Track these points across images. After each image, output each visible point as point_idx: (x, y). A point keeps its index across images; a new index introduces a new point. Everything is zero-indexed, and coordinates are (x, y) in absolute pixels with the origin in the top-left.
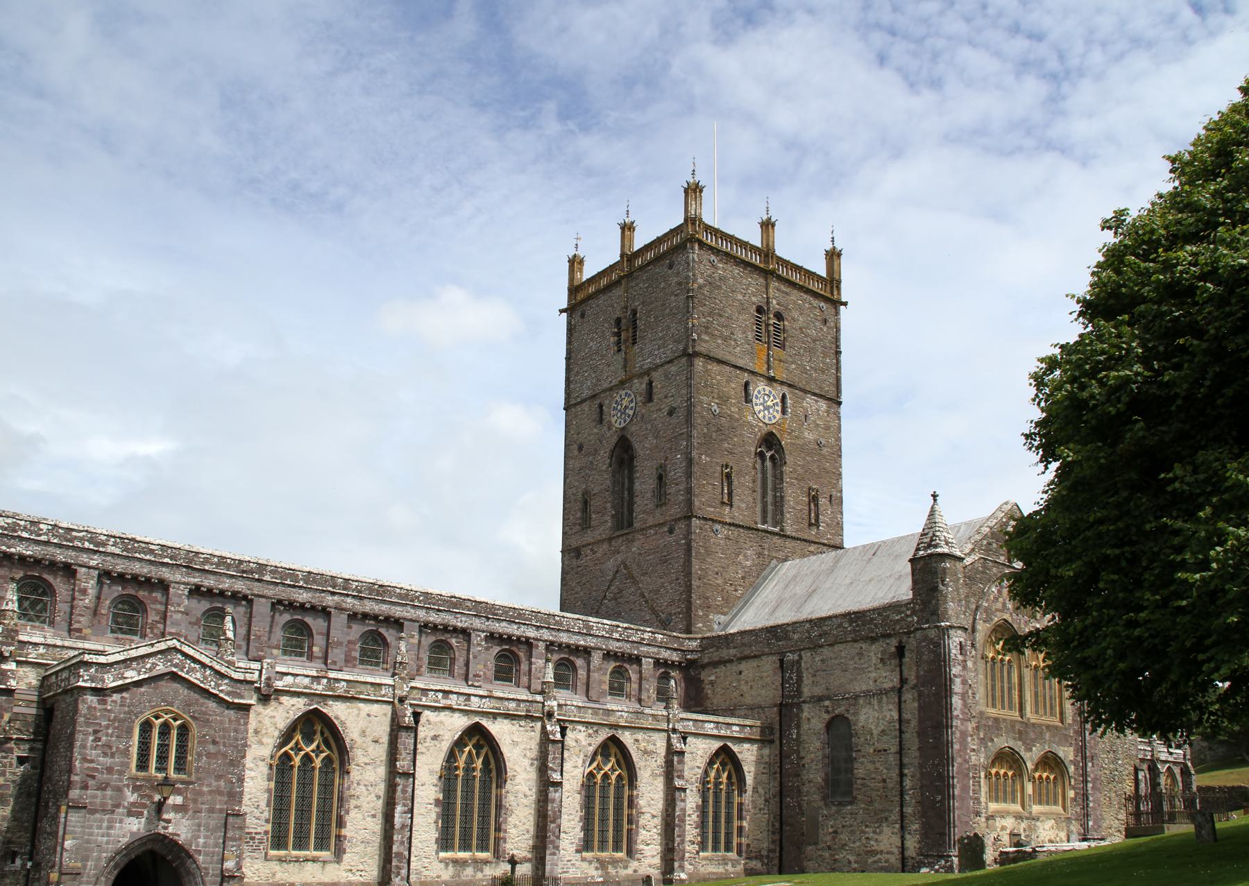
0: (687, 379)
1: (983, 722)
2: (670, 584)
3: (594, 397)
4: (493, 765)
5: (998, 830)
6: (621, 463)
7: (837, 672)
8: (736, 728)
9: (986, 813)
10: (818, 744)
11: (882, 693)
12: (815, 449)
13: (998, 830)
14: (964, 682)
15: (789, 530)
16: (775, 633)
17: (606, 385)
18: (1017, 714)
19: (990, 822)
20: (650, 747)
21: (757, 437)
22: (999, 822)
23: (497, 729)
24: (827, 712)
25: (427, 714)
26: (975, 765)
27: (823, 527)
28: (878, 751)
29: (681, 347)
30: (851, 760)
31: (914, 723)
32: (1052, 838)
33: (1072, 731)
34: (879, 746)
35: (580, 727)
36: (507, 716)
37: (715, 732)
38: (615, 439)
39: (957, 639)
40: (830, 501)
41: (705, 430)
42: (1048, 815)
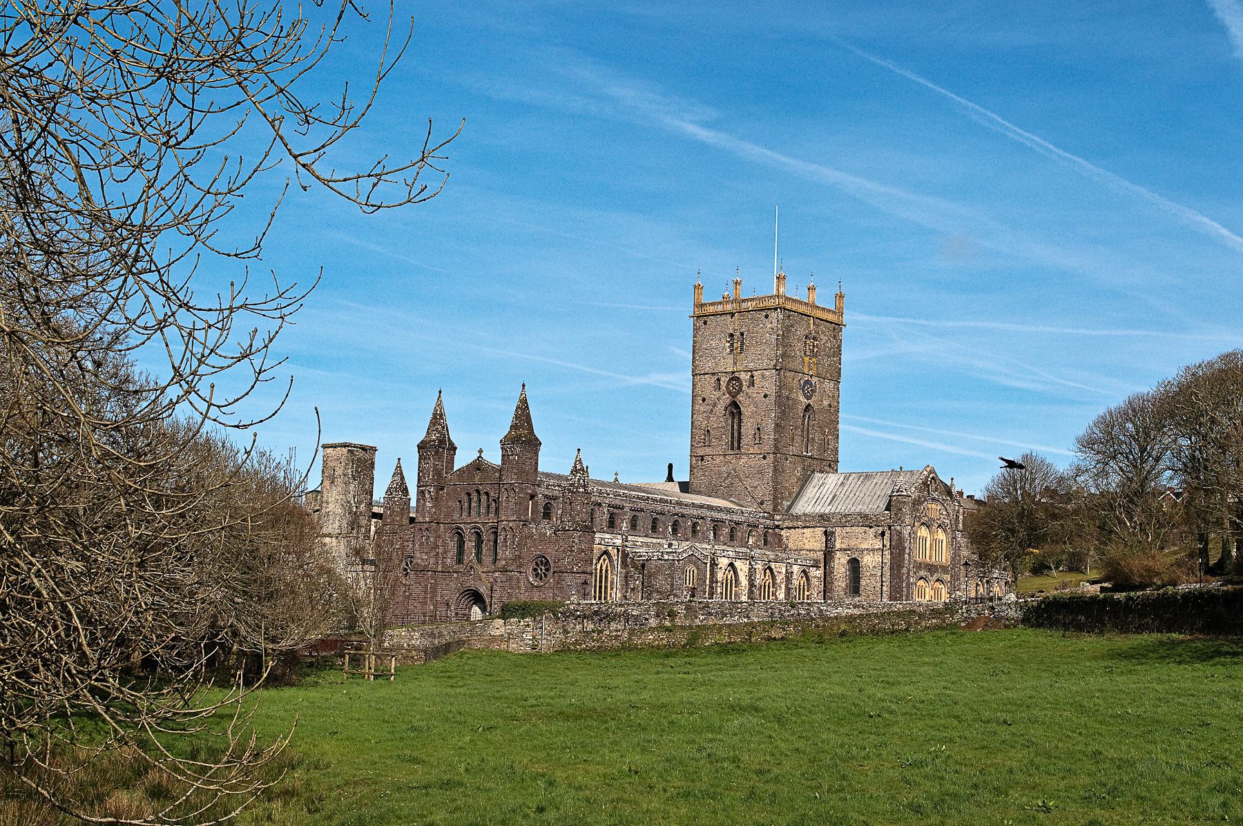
0: (776, 381)
2: (764, 485)
3: (713, 374)
4: (733, 578)
6: (732, 413)
7: (854, 539)
8: (808, 561)
10: (844, 570)
11: (873, 550)
14: (910, 548)
16: (823, 517)
17: (722, 370)
18: (929, 561)
20: (780, 570)
23: (738, 564)
24: (849, 556)
25: (719, 558)
28: (872, 575)
29: (773, 363)
30: (859, 578)
31: (889, 564)
34: (872, 572)
35: (759, 562)
36: (739, 559)
37: (801, 563)
38: (728, 401)
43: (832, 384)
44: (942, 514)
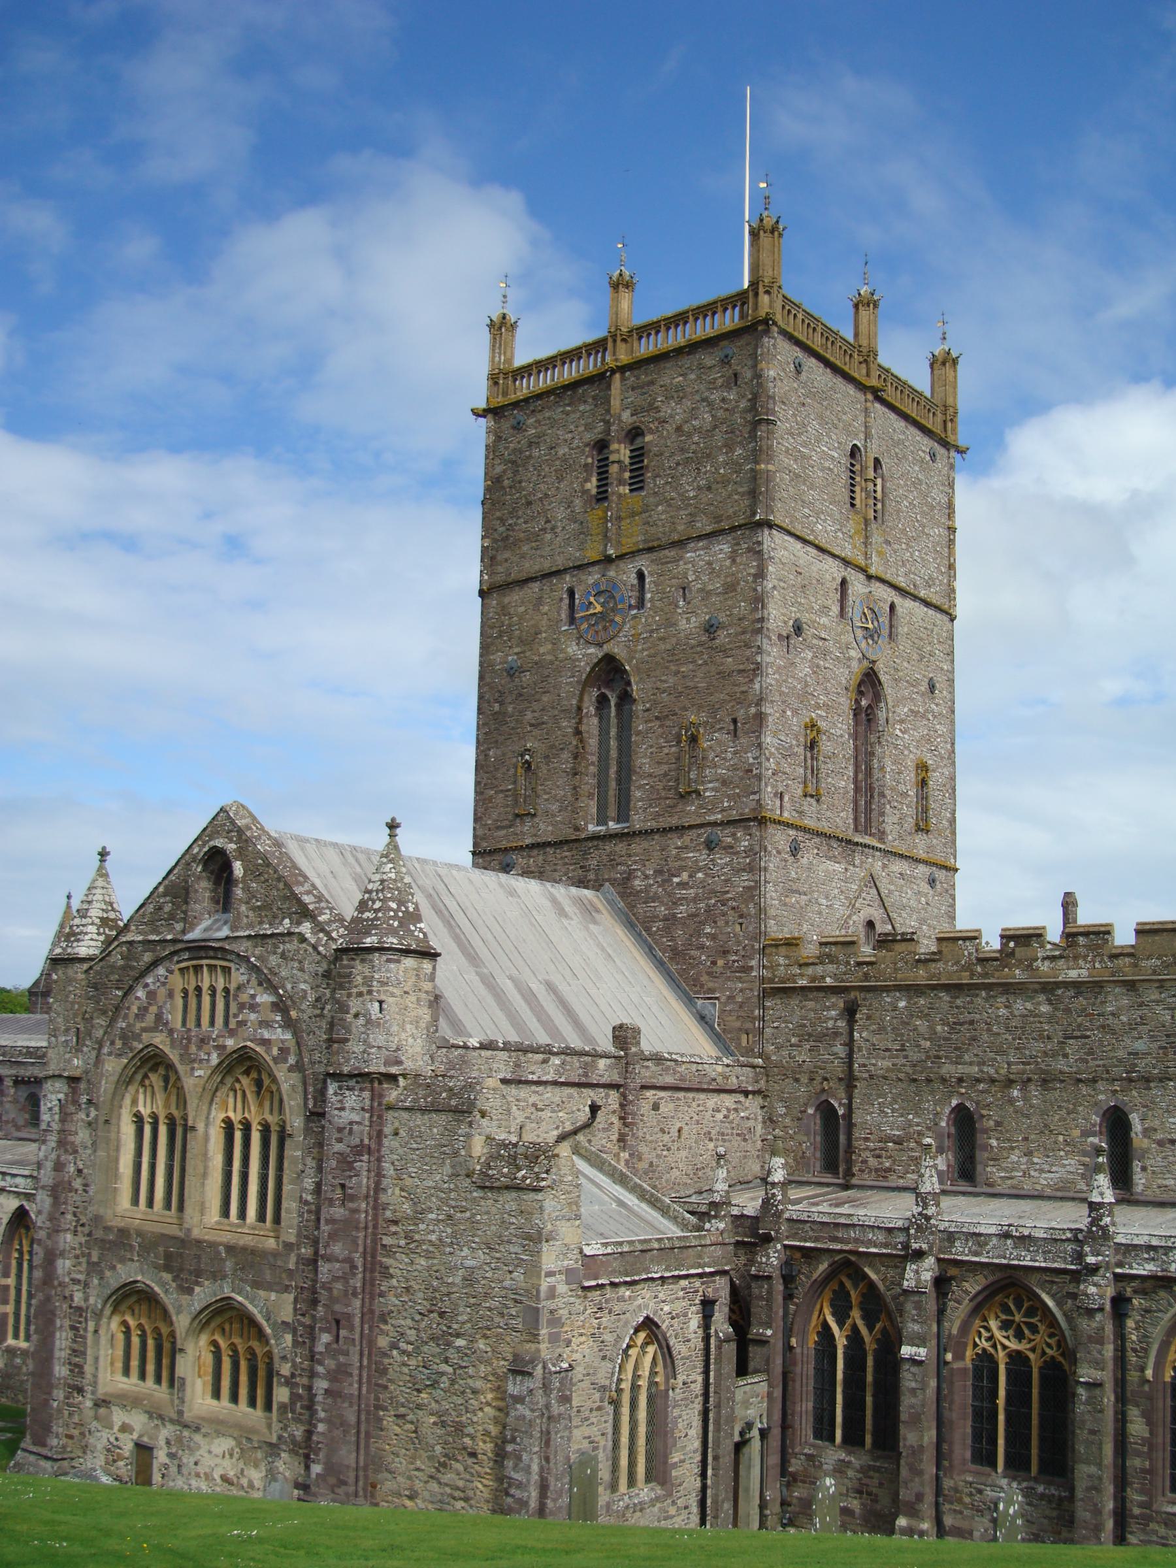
1: (99, 1234)
5: (116, 1428)
9: (93, 1393)
12: (701, 644)
13: (116, 1428)
15: (638, 821)
19: (102, 1411)
21: (584, 676)
22: (119, 1416)
26: (79, 1309)
27: (713, 789)
32: (231, 1474)
33: (293, 1259)
39: (54, 1097)
40: (735, 733)
41: (497, 707)
42: (219, 1426)
43: (722, 548)
44: (253, 1007)
